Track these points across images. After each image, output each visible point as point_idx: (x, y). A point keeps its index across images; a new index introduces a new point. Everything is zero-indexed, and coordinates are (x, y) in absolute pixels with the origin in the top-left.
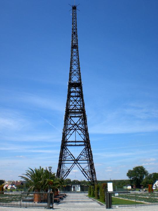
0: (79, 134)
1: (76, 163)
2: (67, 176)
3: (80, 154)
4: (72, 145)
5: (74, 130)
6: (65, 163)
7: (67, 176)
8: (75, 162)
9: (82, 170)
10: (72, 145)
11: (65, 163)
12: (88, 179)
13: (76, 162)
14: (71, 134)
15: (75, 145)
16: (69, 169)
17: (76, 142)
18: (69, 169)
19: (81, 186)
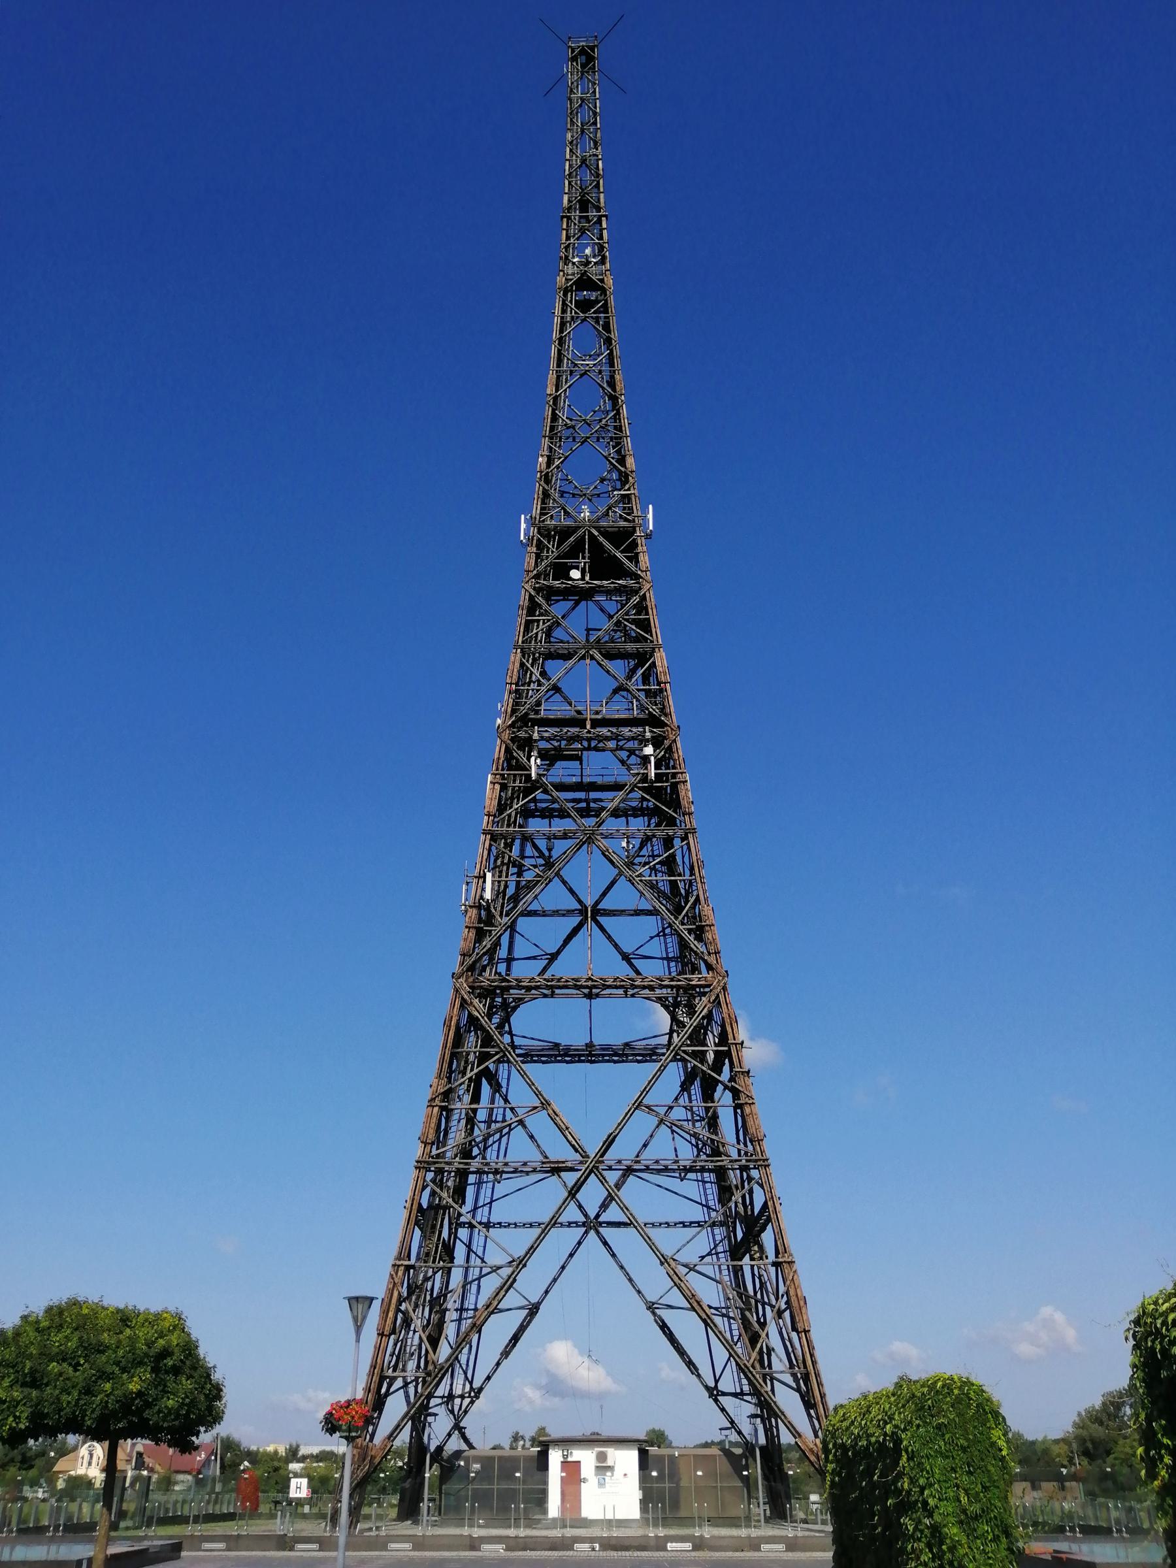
0: (626, 957)
1: (592, 1224)
2: (506, 1353)
3: (638, 1105)
4: (558, 1054)
5: (576, 920)
6: (488, 1225)
7: (506, 1353)
8: (573, 1193)
9: (656, 1283)
10: (558, 1054)
11: (488, 1225)
12: (714, 1393)
13: (593, 1194)
14: (553, 957)
15: (591, 1054)
16: (519, 1252)
17: (591, 990)
18: (520, 1263)
19: (643, 1455)
